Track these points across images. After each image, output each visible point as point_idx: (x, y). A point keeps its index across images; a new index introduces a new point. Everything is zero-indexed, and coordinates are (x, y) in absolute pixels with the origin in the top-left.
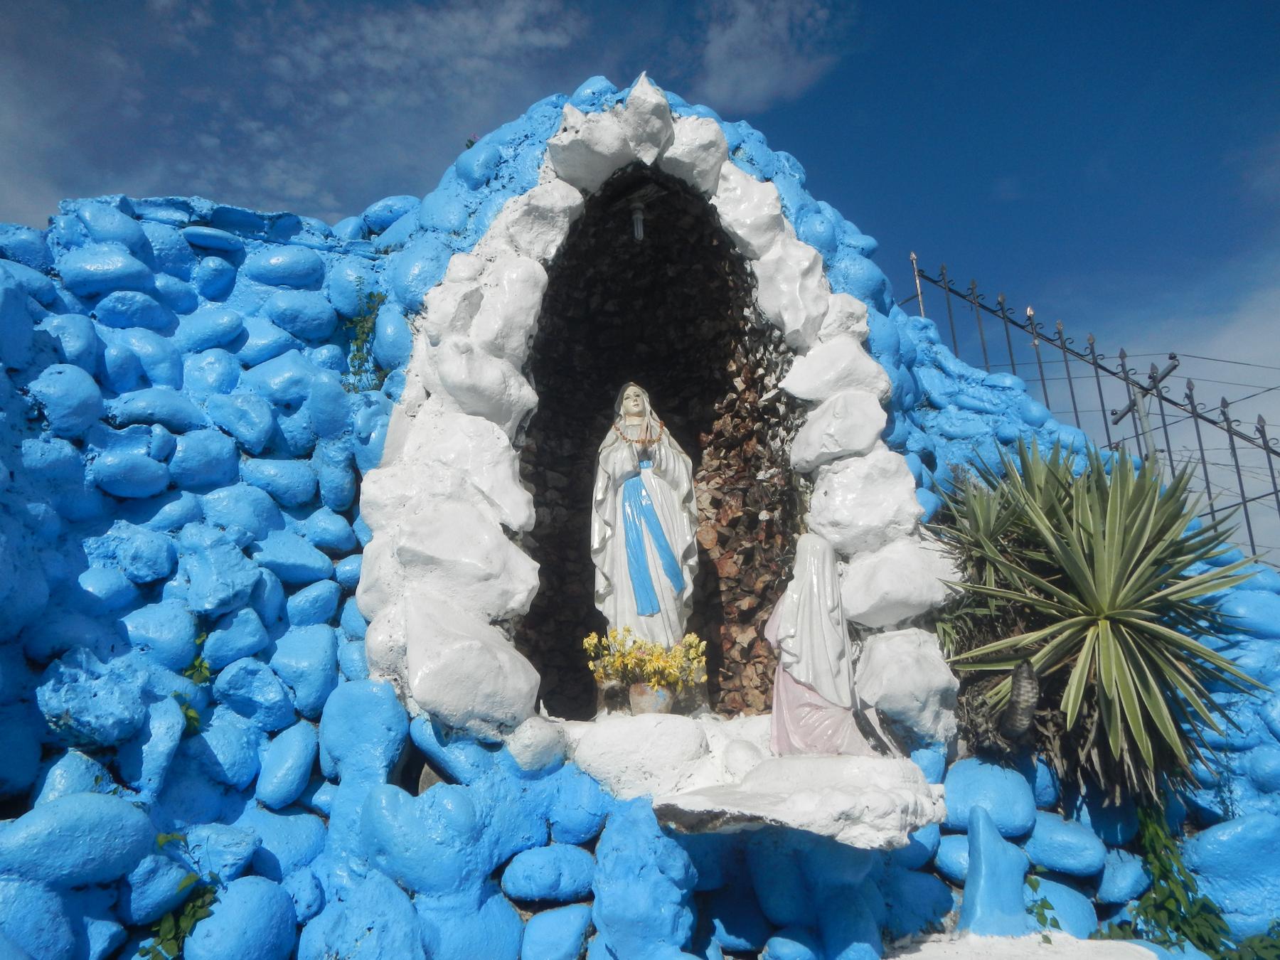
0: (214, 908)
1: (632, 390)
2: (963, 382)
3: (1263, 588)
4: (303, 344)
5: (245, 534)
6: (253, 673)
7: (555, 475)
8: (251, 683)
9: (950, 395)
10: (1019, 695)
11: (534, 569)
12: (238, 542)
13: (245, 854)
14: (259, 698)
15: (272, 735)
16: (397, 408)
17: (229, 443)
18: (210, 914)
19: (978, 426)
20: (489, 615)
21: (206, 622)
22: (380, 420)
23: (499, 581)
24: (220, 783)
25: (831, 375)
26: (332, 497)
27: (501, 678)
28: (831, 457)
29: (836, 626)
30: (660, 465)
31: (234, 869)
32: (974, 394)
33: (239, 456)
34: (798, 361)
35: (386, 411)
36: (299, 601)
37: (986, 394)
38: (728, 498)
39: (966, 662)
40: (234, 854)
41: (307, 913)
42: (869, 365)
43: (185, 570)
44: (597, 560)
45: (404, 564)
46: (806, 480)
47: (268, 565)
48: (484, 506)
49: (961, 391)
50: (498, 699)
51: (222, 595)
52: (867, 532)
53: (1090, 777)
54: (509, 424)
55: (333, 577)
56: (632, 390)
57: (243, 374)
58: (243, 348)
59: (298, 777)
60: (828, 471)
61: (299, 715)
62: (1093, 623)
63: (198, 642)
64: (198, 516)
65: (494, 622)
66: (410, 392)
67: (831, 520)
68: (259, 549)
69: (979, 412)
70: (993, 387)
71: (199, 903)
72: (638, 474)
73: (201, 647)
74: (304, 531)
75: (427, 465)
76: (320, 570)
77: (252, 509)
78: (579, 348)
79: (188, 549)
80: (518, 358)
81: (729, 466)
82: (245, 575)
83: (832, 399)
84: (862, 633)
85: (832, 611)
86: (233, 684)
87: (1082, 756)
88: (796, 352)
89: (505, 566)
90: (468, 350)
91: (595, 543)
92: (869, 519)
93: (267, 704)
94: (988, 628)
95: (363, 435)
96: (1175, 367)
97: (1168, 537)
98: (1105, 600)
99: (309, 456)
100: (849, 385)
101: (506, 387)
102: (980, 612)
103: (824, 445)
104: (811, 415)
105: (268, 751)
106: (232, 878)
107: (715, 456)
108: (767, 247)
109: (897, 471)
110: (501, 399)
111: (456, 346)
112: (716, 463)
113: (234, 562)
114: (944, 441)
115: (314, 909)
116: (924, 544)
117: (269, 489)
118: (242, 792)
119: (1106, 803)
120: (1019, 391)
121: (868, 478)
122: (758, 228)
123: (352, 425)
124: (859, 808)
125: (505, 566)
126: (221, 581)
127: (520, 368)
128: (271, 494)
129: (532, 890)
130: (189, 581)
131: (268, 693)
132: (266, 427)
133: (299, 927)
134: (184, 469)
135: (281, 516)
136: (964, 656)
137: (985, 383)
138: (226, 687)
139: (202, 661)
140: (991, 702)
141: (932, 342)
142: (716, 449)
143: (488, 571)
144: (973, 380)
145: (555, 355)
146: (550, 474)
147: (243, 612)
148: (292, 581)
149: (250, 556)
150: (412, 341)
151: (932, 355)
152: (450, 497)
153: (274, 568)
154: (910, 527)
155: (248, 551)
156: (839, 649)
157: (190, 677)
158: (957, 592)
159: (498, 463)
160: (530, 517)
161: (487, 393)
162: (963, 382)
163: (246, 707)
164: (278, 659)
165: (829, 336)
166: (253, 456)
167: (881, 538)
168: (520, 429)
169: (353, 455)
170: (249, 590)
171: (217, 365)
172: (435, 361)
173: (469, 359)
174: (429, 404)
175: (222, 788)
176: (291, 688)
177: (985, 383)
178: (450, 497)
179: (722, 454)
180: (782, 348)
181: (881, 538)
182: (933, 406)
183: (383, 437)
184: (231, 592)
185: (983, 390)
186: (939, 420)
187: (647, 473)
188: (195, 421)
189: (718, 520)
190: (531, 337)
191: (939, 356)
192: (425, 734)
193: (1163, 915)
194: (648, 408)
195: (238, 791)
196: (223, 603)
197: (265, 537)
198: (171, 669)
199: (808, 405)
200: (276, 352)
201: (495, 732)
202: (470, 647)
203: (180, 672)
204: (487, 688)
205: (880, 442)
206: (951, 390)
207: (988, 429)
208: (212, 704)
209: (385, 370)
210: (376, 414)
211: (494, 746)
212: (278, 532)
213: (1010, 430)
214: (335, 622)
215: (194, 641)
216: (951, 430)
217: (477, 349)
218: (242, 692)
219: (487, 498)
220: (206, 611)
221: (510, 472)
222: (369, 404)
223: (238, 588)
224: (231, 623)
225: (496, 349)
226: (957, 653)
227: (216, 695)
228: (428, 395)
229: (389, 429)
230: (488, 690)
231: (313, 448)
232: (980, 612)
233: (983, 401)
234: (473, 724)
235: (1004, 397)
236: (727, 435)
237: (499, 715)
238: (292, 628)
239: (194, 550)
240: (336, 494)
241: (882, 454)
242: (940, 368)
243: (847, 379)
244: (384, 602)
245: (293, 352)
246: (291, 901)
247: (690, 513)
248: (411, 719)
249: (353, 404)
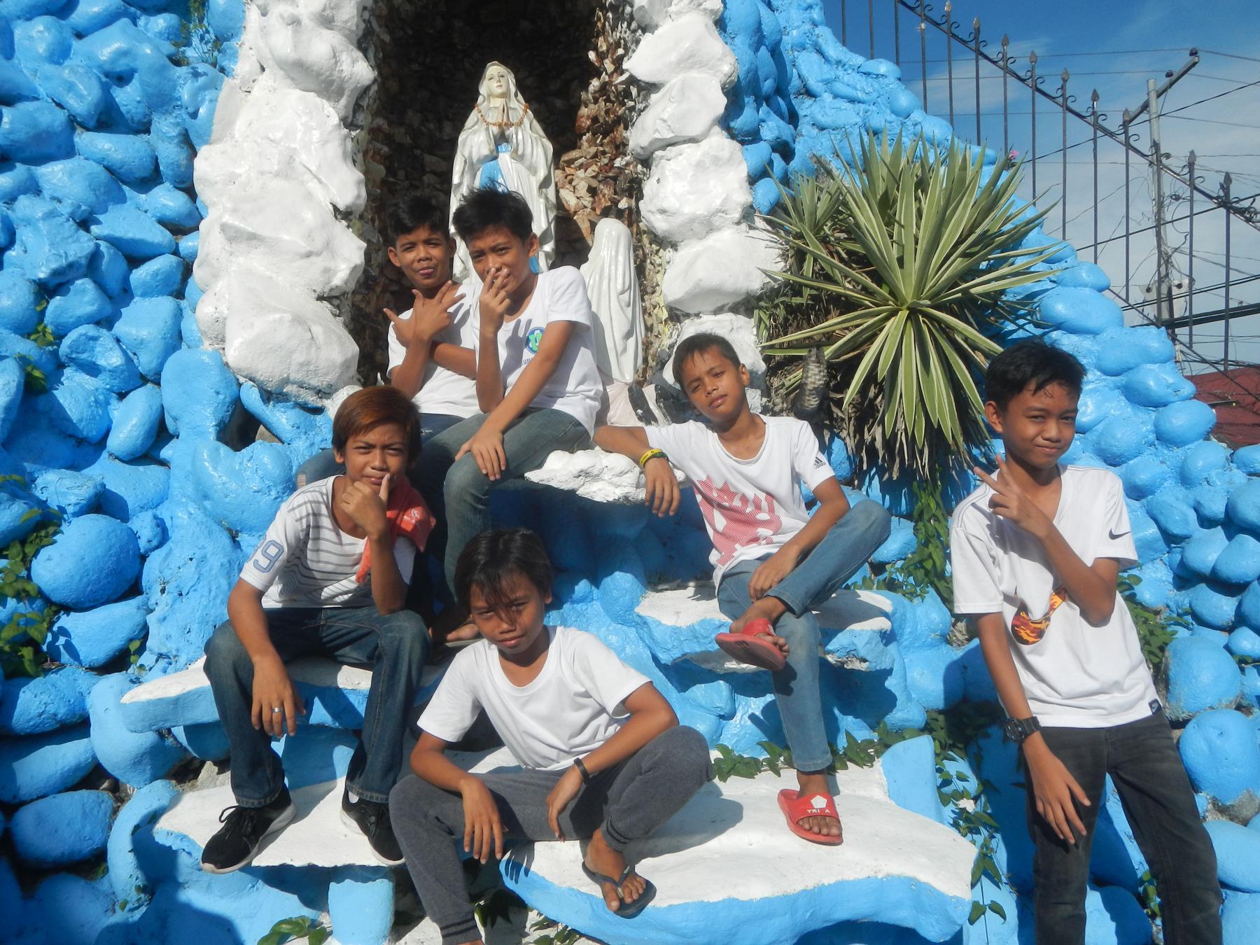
0: (57, 537)
1: (494, 70)
2: (840, 68)
3: (1086, 286)
4: (139, 12)
5: (80, 206)
6: (95, 339)
7: (434, 159)
8: (93, 349)
9: (827, 82)
10: (807, 378)
11: (360, 248)
12: (72, 216)
13: (87, 496)
14: (101, 362)
15: (122, 396)
16: (228, 83)
17: (60, 117)
18: (55, 542)
19: (849, 115)
20: (315, 291)
21: (46, 290)
22: (208, 95)
23: (321, 258)
24: (71, 436)
25: (673, 57)
26: (170, 173)
27: (314, 349)
28: (664, 143)
29: (625, 308)
30: (516, 151)
31: (77, 508)
32: (850, 82)
33: (73, 129)
34: (647, 39)
35: (214, 85)
36: (140, 275)
37: (861, 82)
38: (601, 187)
39: (772, 347)
40: (77, 495)
41: (148, 546)
42: (715, 45)
43: (22, 241)
45: (231, 240)
46: (643, 166)
47: (107, 239)
48: (313, 185)
49: (837, 78)
50: (312, 368)
51: (54, 266)
52: (693, 220)
53: (872, 451)
54: (343, 101)
55: (176, 252)
56: (494, 70)
57: (76, 44)
58: (74, 15)
59: (143, 433)
60: (662, 157)
61: (144, 380)
62: (894, 313)
63: (39, 309)
64: (33, 188)
65: (320, 298)
66: (243, 66)
67: (659, 207)
68: (98, 222)
69: (852, 101)
70: (867, 74)
71: (43, 533)
72: (495, 158)
73: (43, 313)
74: (146, 207)
75: (256, 142)
76: (159, 245)
77: (87, 183)
78: (458, 24)
79: (22, 220)
80: (352, 31)
81: (604, 153)
82: (80, 247)
83: (674, 81)
84: (681, 318)
85: (623, 292)
86: (74, 347)
87: (867, 437)
88: (644, 31)
89: (328, 245)
90: (295, 22)
92: (694, 207)
93: (109, 368)
94: (799, 316)
95: (191, 110)
96: (1195, 64)
97: (979, 231)
98: (907, 290)
99: (147, 131)
100: (691, 68)
101: (336, 63)
102: (797, 300)
103: (657, 130)
104: (654, 97)
105: (117, 411)
106: (77, 514)
107: (592, 143)
109: (730, 159)
110: (331, 75)
111: (282, 17)
112: (593, 150)
113: (67, 234)
114: (815, 131)
115: (155, 543)
116: (752, 233)
117: (105, 163)
118: (95, 445)
119: (887, 476)
120: (892, 79)
121: (700, 166)
123: (179, 99)
124: (598, 467)
125: (328, 245)
126: (53, 251)
127: (355, 42)
128: (108, 168)
130: (26, 252)
131: (111, 359)
132: (95, 101)
133: (143, 558)
134: (12, 141)
135: (121, 190)
136: (774, 342)
137: (861, 70)
138: (68, 351)
139: (45, 327)
140: (787, 384)
141: (815, 24)
142: (594, 134)
143: (309, 249)
144: (850, 66)
145: (432, 31)
146: (428, 159)
147: (79, 282)
148: (135, 256)
149: (88, 230)
150: (244, 12)
151: (814, 38)
152: (277, 175)
153: (114, 242)
154: (737, 215)
155: (84, 224)
156: (626, 329)
157: (35, 340)
158: (775, 280)
159: (326, 142)
160: (358, 197)
161: (315, 68)
162: (840, 68)
163: (92, 369)
164: (120, 328)
165: (679, 13)
166: (88, 130)
167: (708, 226)
168: (357, 107)
169: (186, 130)
170: (84, 261)
171: (46, 34)
172: (265, 32)
173: (296, 32)
174: (265, 80)
175: (73, 441)
176: (135, 354)
177: (861, 70)
178: (277, 175)
179: (598, 141)
180: (634, 25)
181: (708, 226)
182: (810, 94)
183: (211, 113)
184: (64, 262)
185: (858, 77)
186: (813, 108)
187: (505, 158)
188: (26, 93)
189: (594, 209)
190: (365, 8)
191: (820, 40)
192: (251, 399)
193: (921, 573)
194: (513, 89)
195: (90, 444)
196: (56, 273)
197: (106, 211)
198: (16, 333)
199: (651, 88)
200: (107, 20)
201: (314, 398)
202: (281, 319)
203: (27, 335)
204: (299, 357)
205: (717, 129)
206: (827, 76)
207: (858, 120)
208: (61, 366)
209: (222, 41)
210: (204, 88)
211: (318, 411)
212: (119, 206)
213: (877, 121)
214: (180, 294)
215: (35, 310)
216: (824, 120)
217: (306, 21)
218: (84, 356)
219: (316, 177)
220: (40, 279)
221: (340, 151)
222: (196, 75)
223: (71, 259)
224: (69, 290)
225: (326, 21)
226: (770, 338)
227: (63, 359)
228: (263, 69)
229: (218, 105)
230: (301, 359)
231: (150, 123)
232: (797, 300)
233: (856, 89)
235: (876, 86)
236: (601, 120)
237: (315, 382)
238: (136, 299)
239: (28, 222)
240: (173, 170)
241: (719, 142)
242: (820, 52)
243: (690, 61)
244: (216, 276)
245: (124, 21)
246: (134, 536)
247: (547, 199)
248: (240, 385)
249: (179, 77)
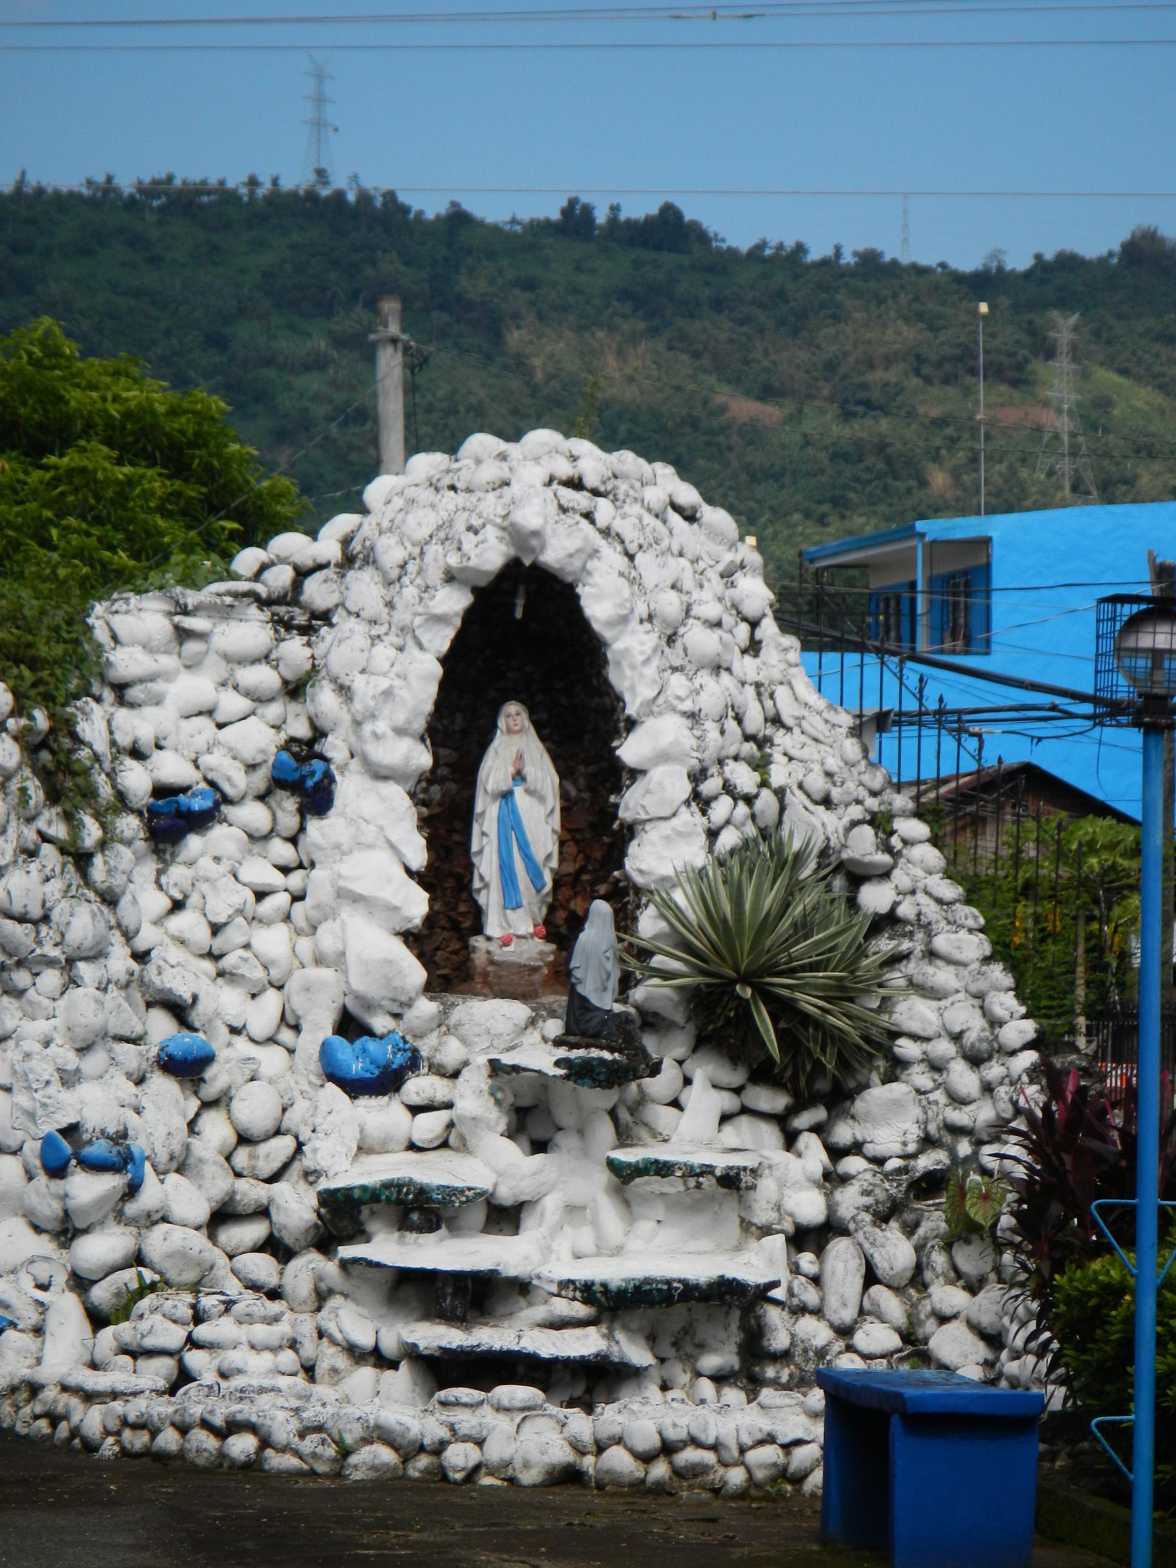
1: (513, 714)
9: (797, 718)
44: (475, 860)
91: (475, 847)
108: (616, 639)
114: (785, 759)
122: (611, 624)
129: (416, 1100)
196: (229, 917)
216: (794, 752)
228: (352, 756)
234: (385, 1003)
237: (404, 998)
243: (664, 757)
